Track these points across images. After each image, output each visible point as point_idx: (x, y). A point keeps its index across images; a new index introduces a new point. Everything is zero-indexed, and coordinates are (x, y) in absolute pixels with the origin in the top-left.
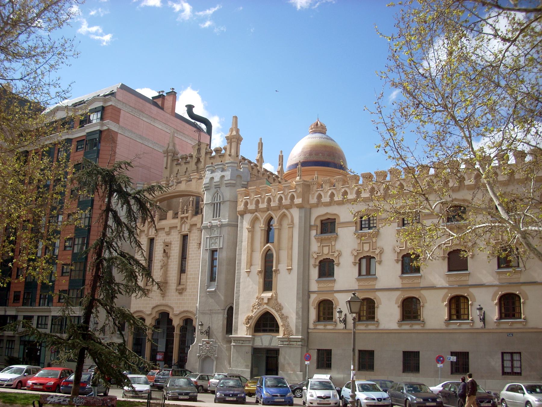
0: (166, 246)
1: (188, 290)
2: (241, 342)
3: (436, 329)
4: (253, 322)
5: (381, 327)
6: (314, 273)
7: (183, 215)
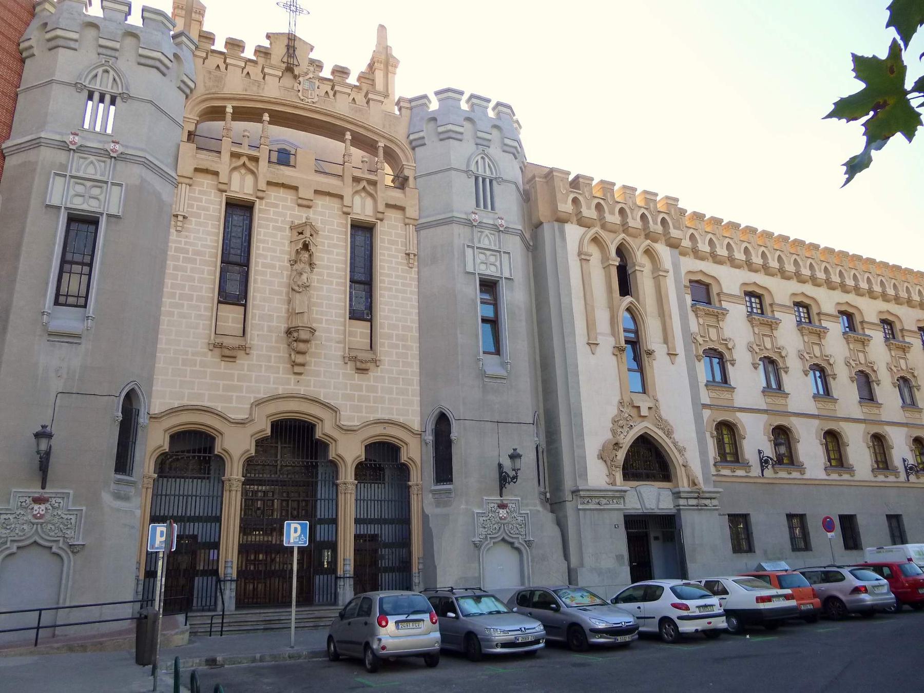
1: (385, 366)
2: (604, 501)
3: (867, 481)
4: (621, 455)
5: (807, 476)
6: (702, 371)
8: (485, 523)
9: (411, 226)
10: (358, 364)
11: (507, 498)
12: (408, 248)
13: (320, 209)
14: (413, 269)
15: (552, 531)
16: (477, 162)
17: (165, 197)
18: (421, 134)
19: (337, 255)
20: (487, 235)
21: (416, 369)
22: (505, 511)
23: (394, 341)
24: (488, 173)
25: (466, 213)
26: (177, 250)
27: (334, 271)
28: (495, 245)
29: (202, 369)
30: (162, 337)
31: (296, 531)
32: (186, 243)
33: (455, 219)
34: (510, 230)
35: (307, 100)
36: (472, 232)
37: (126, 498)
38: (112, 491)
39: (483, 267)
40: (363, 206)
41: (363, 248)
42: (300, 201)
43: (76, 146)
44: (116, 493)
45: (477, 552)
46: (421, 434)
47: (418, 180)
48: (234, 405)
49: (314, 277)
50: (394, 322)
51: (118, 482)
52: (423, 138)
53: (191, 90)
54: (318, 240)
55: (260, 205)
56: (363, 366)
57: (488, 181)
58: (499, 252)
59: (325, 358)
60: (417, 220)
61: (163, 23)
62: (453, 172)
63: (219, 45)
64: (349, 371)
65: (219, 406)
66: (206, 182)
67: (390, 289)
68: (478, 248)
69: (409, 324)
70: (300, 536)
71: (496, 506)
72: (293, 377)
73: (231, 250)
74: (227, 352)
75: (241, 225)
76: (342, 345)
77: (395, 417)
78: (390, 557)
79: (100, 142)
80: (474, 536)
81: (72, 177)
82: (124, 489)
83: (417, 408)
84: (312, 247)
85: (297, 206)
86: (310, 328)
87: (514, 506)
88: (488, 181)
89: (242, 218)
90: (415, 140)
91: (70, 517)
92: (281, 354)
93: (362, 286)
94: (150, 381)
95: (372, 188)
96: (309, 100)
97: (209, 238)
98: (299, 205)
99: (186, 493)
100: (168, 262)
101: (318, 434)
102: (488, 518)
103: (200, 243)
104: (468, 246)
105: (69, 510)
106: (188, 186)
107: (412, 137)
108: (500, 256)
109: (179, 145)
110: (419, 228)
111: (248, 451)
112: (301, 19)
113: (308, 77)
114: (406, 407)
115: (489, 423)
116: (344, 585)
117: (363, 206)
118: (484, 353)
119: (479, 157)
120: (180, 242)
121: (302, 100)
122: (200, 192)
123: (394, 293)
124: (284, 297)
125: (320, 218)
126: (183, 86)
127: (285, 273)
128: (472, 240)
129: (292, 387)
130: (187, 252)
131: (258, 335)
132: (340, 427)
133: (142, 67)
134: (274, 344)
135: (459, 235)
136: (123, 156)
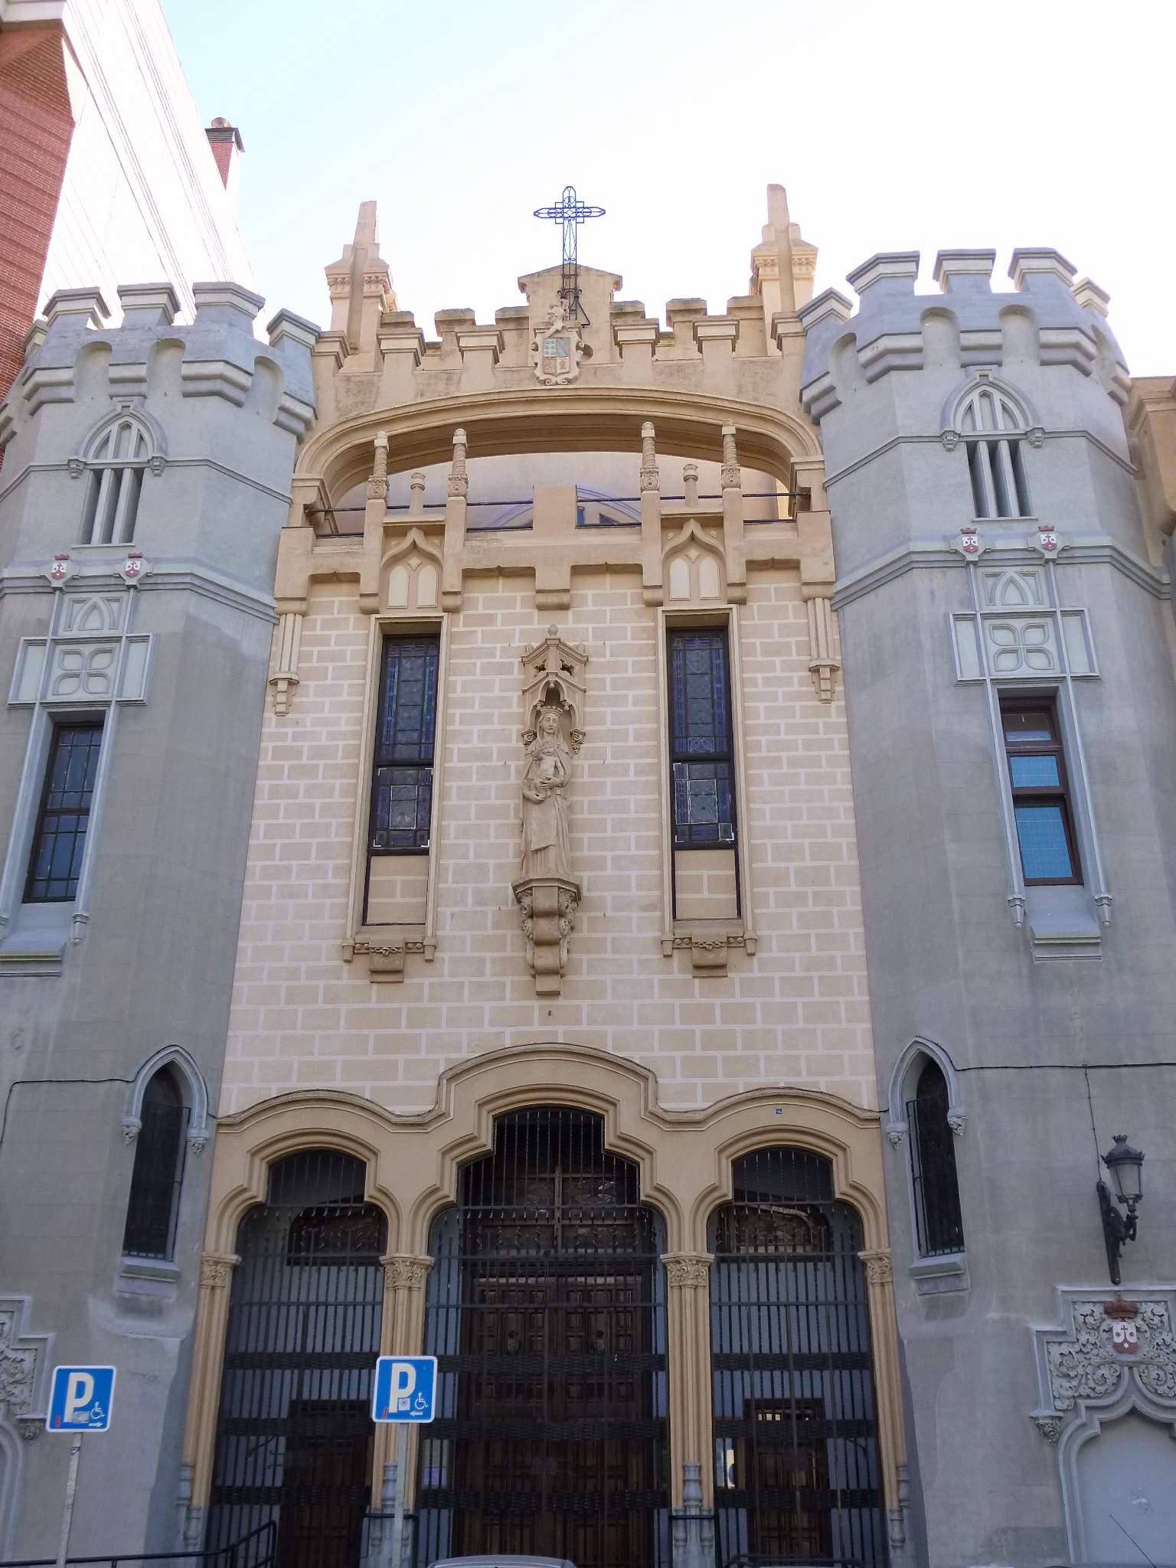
0: (564, 668)
1: (772, 950)
8: (1067, 1360)
9: (819, 601)
10: (698, 956)
11: (1136, 1286)
12: (815, 655)
13: (590, 607)
14: (834, 704)
16: (970, 408)
18: (825, 383)
19: (635, 704)
20: (1012, 581)
21: (856, 949)
22: (1130, 1326)
23: (793, 888)
24: (1003, 426)
25: (945, 538)
27: (631, 742)
28: (1039, 600)
29: (330, 1006)
31: (404, 1378)
32: (296, 736)
33: (915, 558)
34: (1077, 553)
35: (554, 379)
36: (969, 583)
37: (153, 1311)
38: (117, 1294)
39: (1007, 662)
40: (694, 579)
41: (707, 678)
42: (542, 599)
43: (64, 580)
44: (128, 1300)
45: (1047, 1450)
46: (878, 1120)
47: (831, 490)
48: (400, 1082)
49: (580, 762)
50: (790, 840)
51: (131, 1273)
52: (831, 389)
53: (307, 424)
54: (588, 676)
55: (452, 624)
56: (710, 958)
57: (1004, 450)
58: (1051, 614)
59: (615, 950)
60: (831, 583)
61: (233, 305)
62: (905, 448)
64: (677, 976)
65: (366, 1088)
66: (337, 599)
67: (775, 762)
68: (986, 616)
69: (830, 839)
70: (413, 1397)
71: (1098, 1310)
72: (537, 1004)
73: (399, 735)
74: (380, 962)
75: (420, 677)
76: (657, 914)
77: (803, 1080)
78: (270, 1459)
79: (108, 563)
80: (1036, 1404)
81: (56, 642)
82: (146, 1291)
83: (863, 1050)
84: (566, 696)
85: (536, 612)
86: (559, 880)
87: (1160, 1309)
88: (1004, 450)
89: (420, 661)
90: (816, 399)
91: (20, 1355)
92: (509, 953)
93: (709, 768)
94: (218, 1043)
95: (714, 533)
96: (559, 379)
97: (344, 716)
98: (541, 608)
99: (303, 1299)
100: (259, 782)
101: (610, 1140)
102: (1077, 1347)
103: (324, 730)
104: (958, 618)
105: (22, 1340)
106: (299, 618)
107: (806, 397)
108: (1056, 624)
109: (279, 536)
110: (839, 603)
111: (436, 1190)
112: (587, 229)
113: (553, 329)
114: (834, 1052)
115: (1059, 1070)
116: (686, 1540)
117: (694, 579)
118: (1029, 883)
119: (975, 396)
120: (283, 737)
121: (544, 382)
122: (326, 625)
123: (785, 770)
124: (512, 821)
125: (590, 626)
126: (284, 418)
127: (513, 765)
128: (969, 602)
129: (536, 1027)
130: (297, 753)
131: (452, 915)
132: (657, 1118)
133: (192, 400)
134: (490, 932)
135: (932, 593)
136: (151, 581)
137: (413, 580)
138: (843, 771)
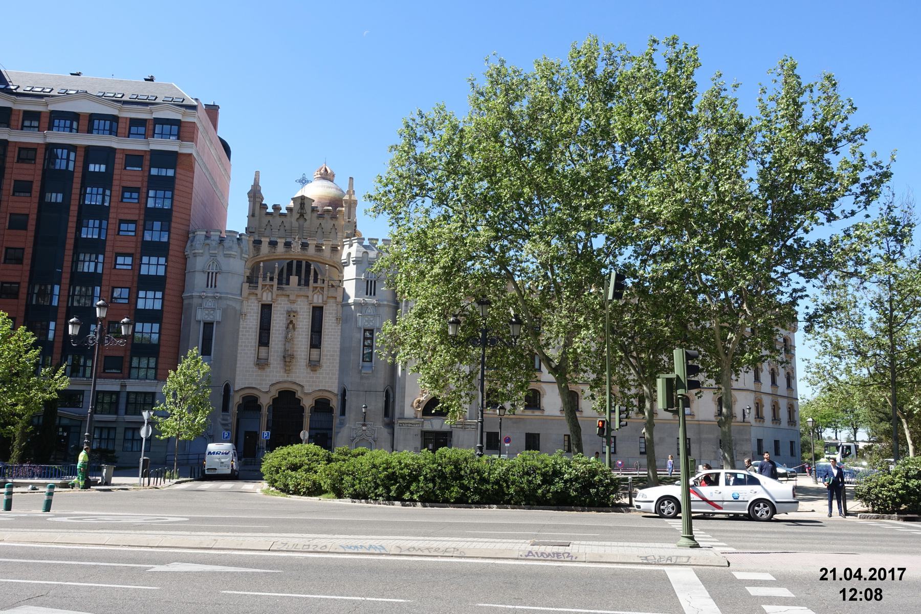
7: (315, 285)
15: (389, 437)
17: (238, 308)
21: (337, 368)
26: (243, 328)
30: (238, 362)
63: (270, 210)
65: (258, 387)
77: (327, 389)
83: (336, 384)
94: (234, 379)
137: (267, 294)
138: (339, 337)
